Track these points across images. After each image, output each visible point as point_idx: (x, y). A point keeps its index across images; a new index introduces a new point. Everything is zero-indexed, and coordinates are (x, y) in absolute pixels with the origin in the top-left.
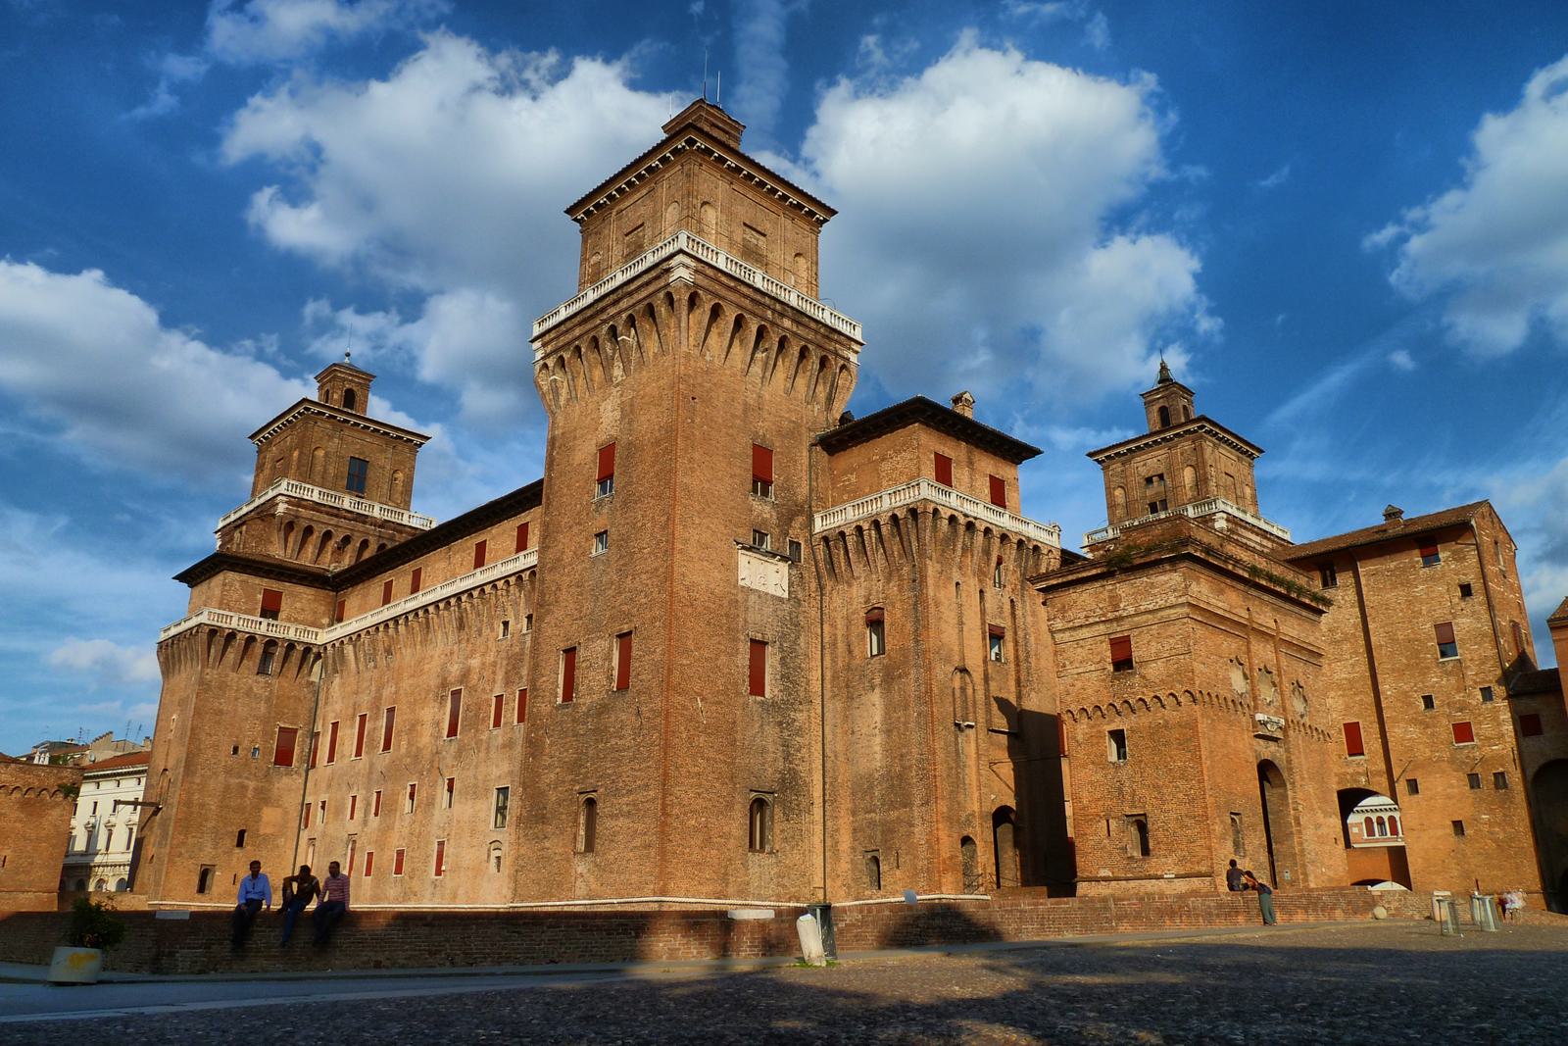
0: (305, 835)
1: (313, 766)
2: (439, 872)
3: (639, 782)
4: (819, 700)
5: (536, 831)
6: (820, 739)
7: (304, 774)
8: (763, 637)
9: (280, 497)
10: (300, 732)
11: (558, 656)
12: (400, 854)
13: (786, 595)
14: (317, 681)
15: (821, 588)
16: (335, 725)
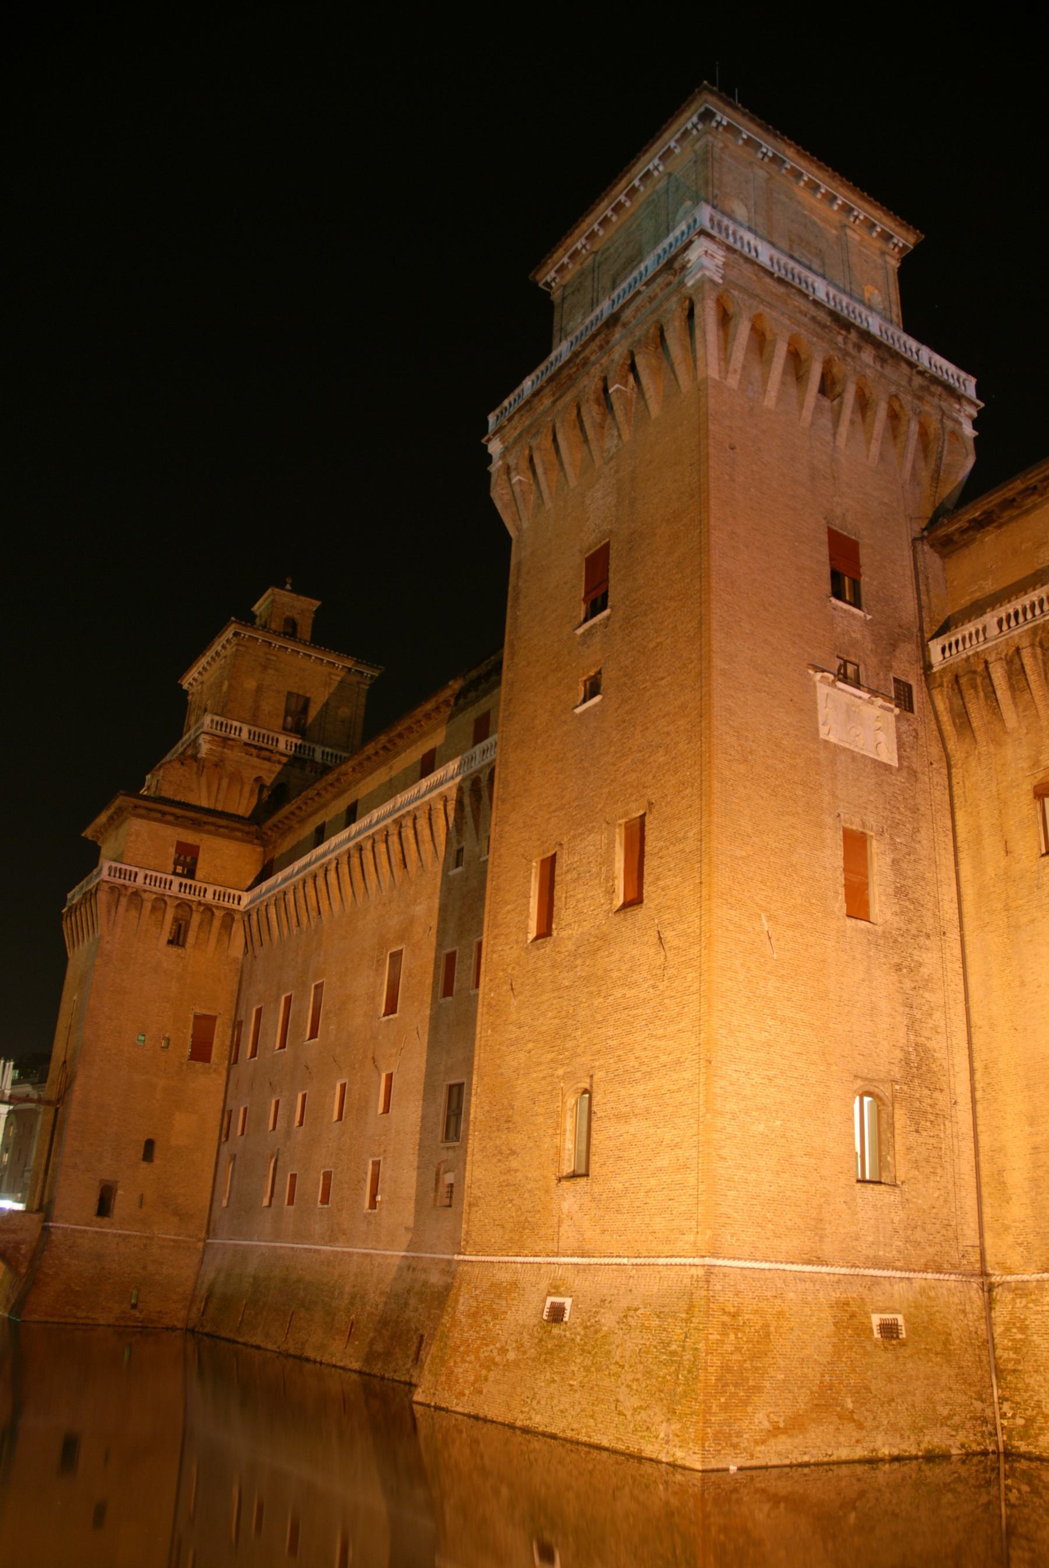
0: (225, 1149)
1: (236, 1062)
2: (373, 1204)
3: (663, 1059)
4: (954, 935)
5: (498, 1142)
6: (962, 997)
7: (224, 1073)
8: (864, 825)
9: (203, 736)
10: (218, 1021)
11: (530, 870)
12: (327, 1176)
13: (895, 764)
14: (241, 956)
15: (948, 757)
16: (259, 1012)
